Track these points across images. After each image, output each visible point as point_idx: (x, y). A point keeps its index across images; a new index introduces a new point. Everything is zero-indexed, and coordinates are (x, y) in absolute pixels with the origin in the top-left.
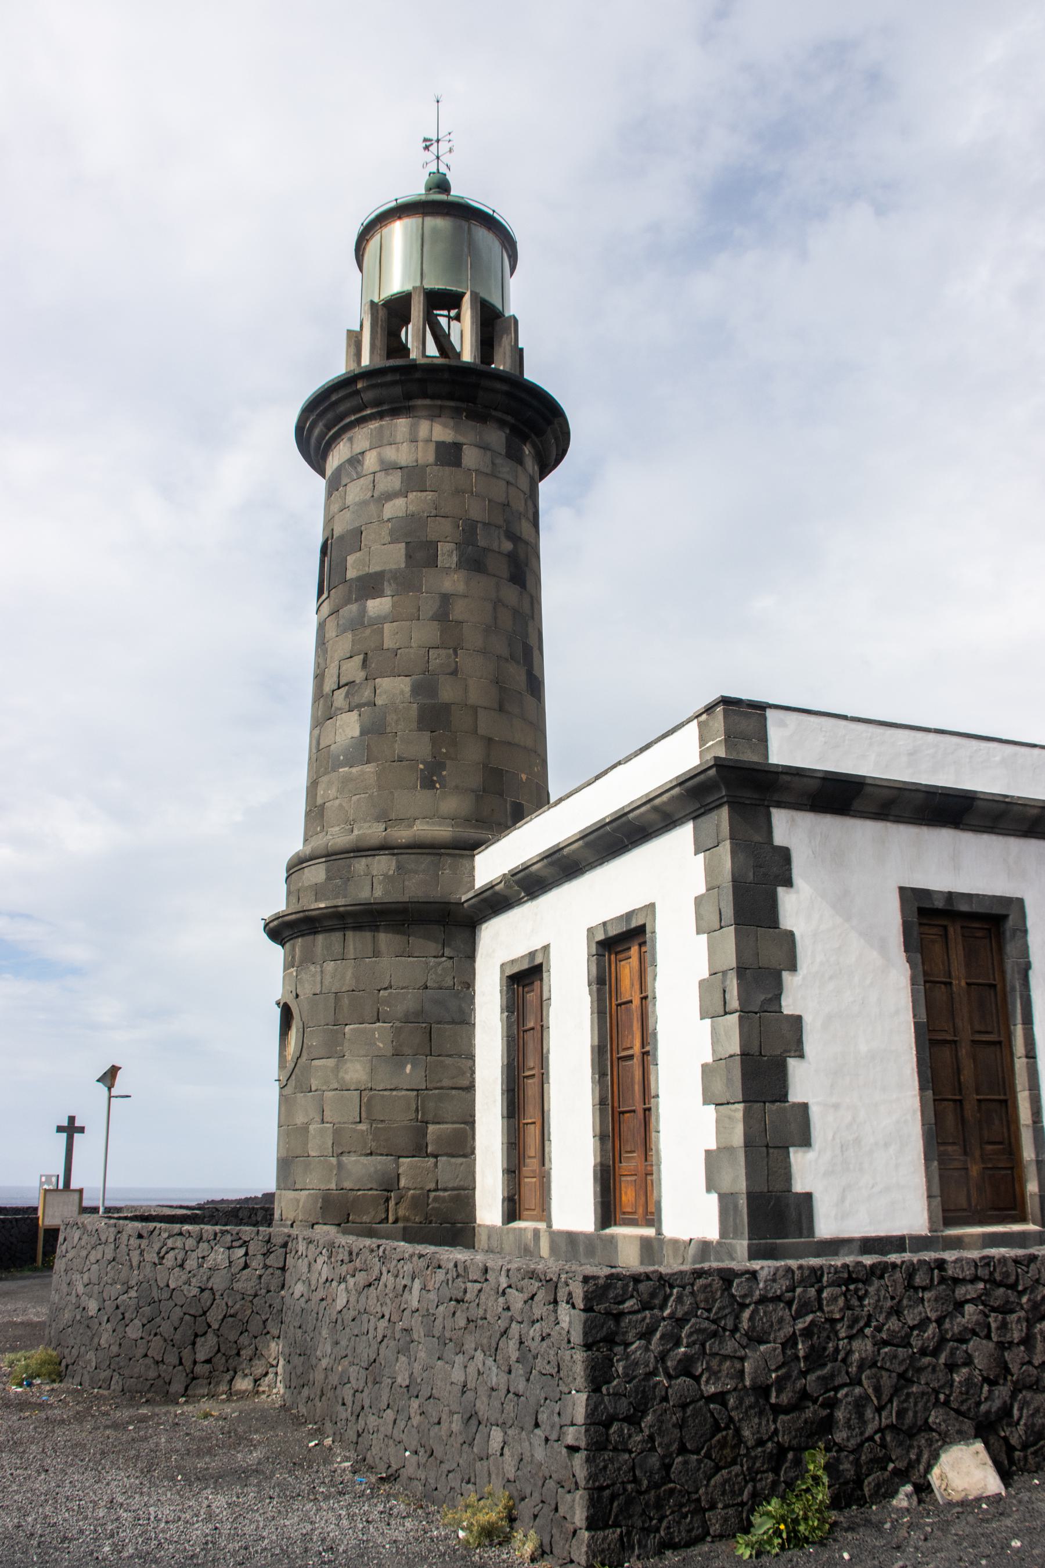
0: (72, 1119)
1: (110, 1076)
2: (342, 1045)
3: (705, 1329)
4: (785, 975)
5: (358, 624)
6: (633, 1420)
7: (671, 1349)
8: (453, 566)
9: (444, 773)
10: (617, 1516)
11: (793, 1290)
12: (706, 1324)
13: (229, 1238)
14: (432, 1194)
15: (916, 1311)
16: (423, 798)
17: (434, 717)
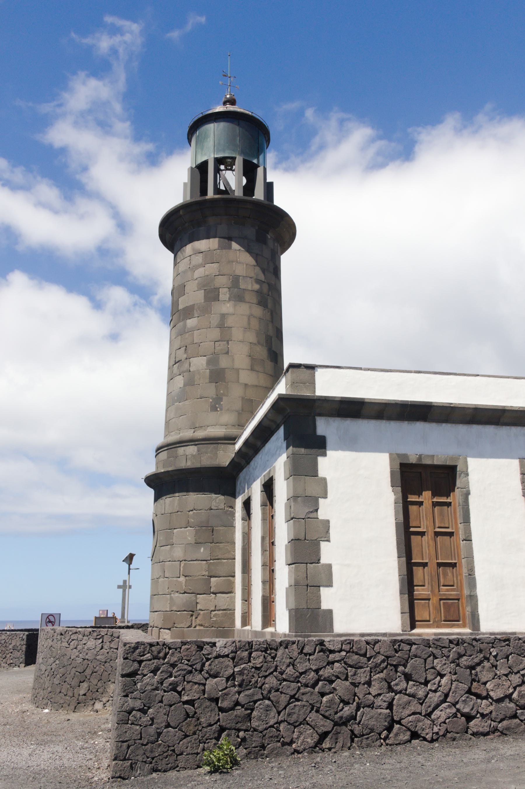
1: (130, 558)
2: (172, 539)
3: (185, 670)
4: (321, 501)
6: (144, 711)
7: (166, 678)
8: (228, 299)
9: (222, 403)
10: (130, 755)
11: (236, 652)
12: (186, 667)
13: (95, 634)
14: (213, 613)
15: (304, 665)
16: (212, 417)
17: (217, 376)
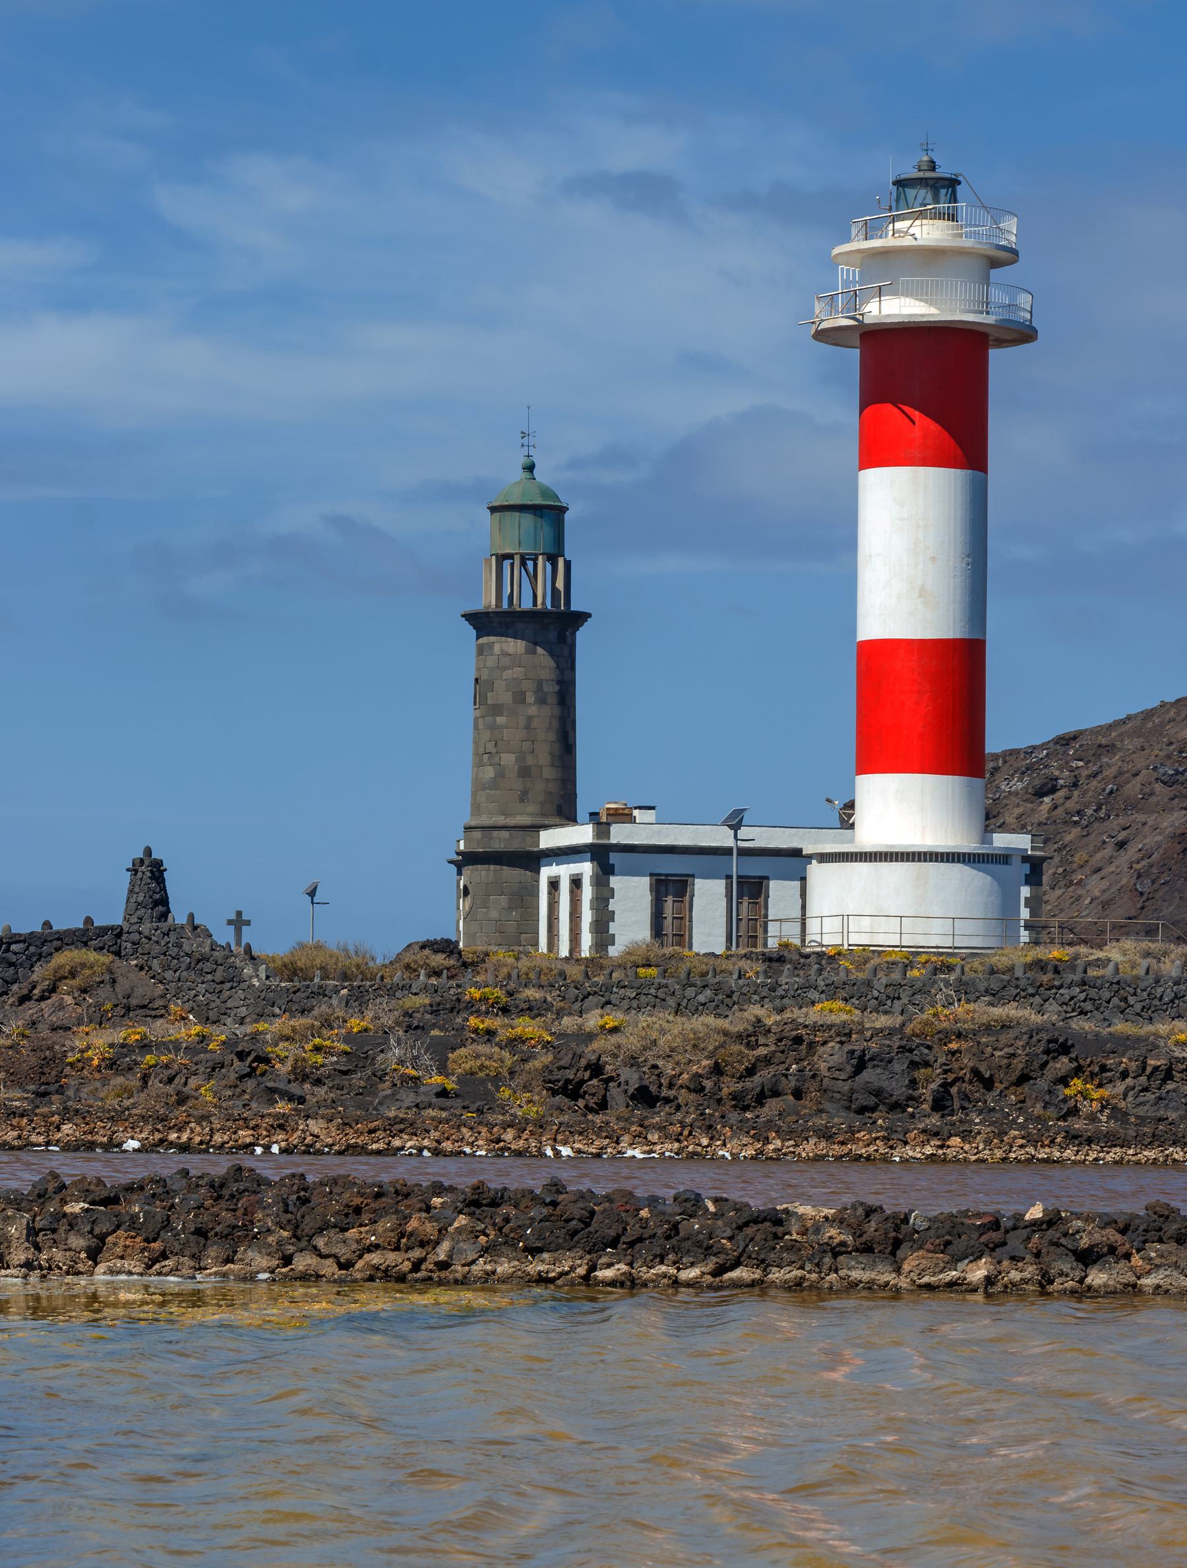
0: (239, 914)
5: (493, 727)
17: (524, 772)
